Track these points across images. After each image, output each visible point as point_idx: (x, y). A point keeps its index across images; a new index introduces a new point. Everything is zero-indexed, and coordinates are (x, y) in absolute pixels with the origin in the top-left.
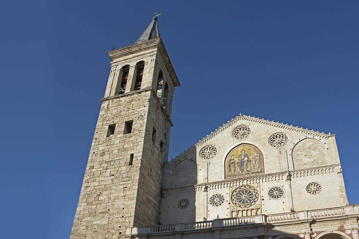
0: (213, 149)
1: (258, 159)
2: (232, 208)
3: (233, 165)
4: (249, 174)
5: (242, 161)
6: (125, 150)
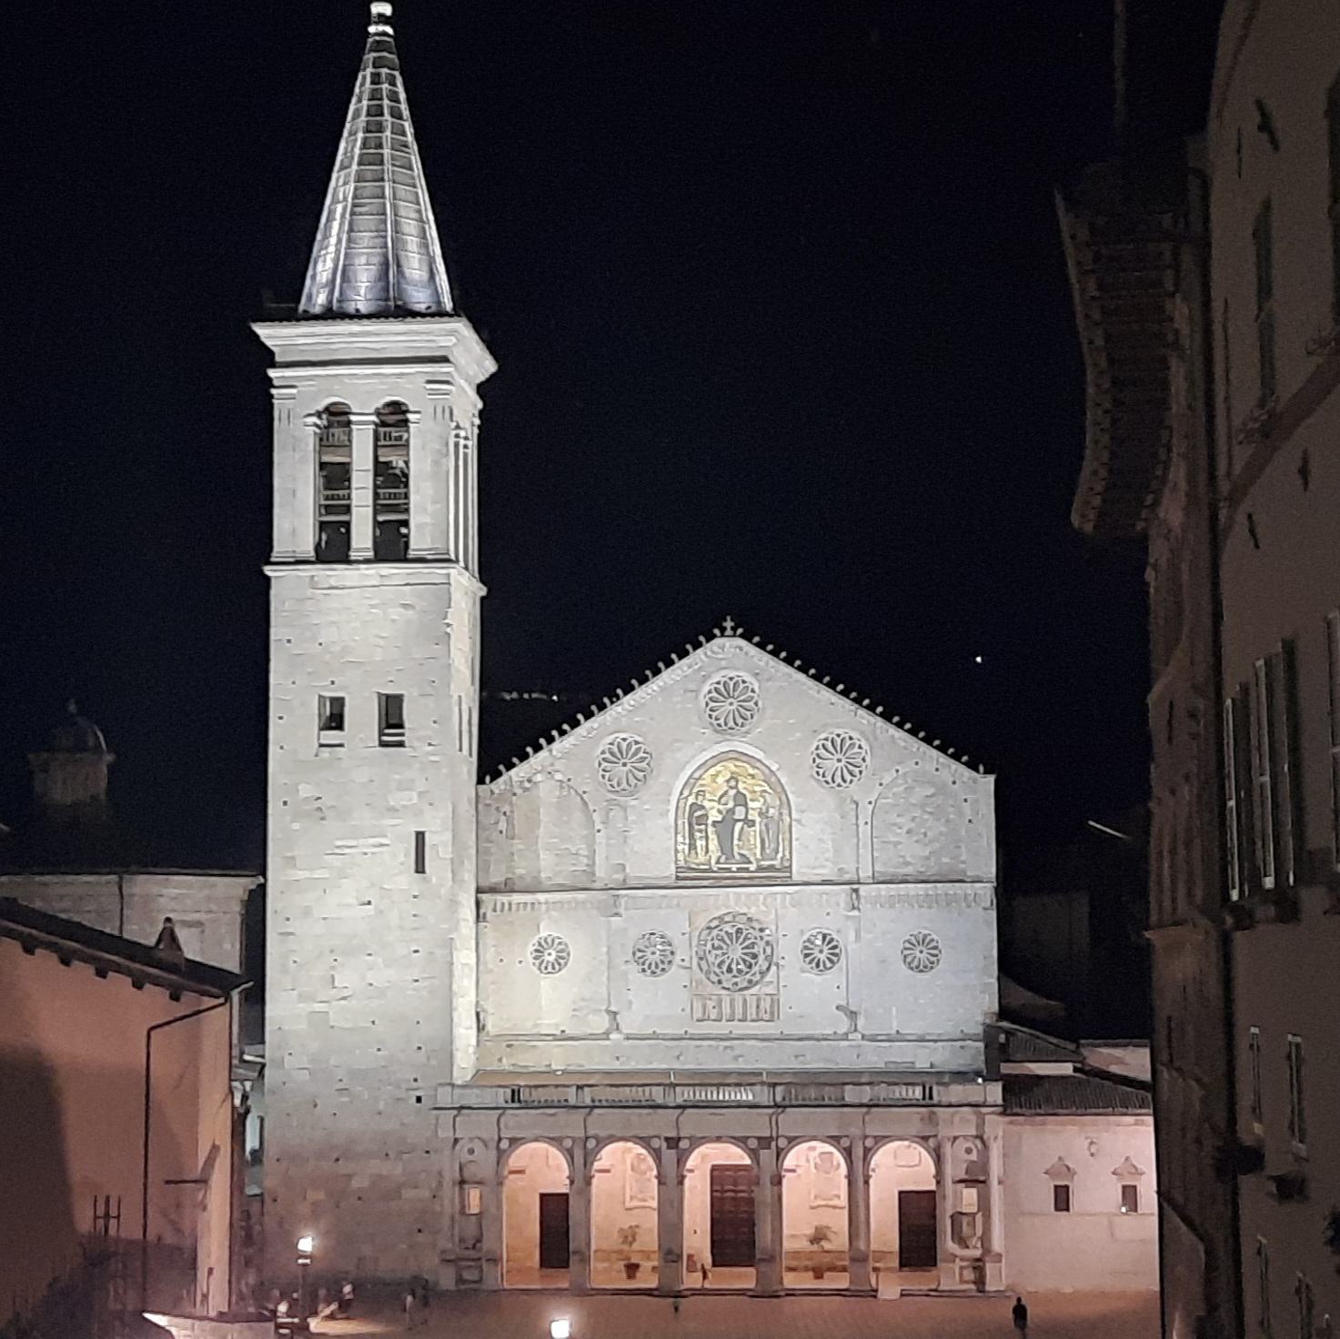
4: (747, 870)
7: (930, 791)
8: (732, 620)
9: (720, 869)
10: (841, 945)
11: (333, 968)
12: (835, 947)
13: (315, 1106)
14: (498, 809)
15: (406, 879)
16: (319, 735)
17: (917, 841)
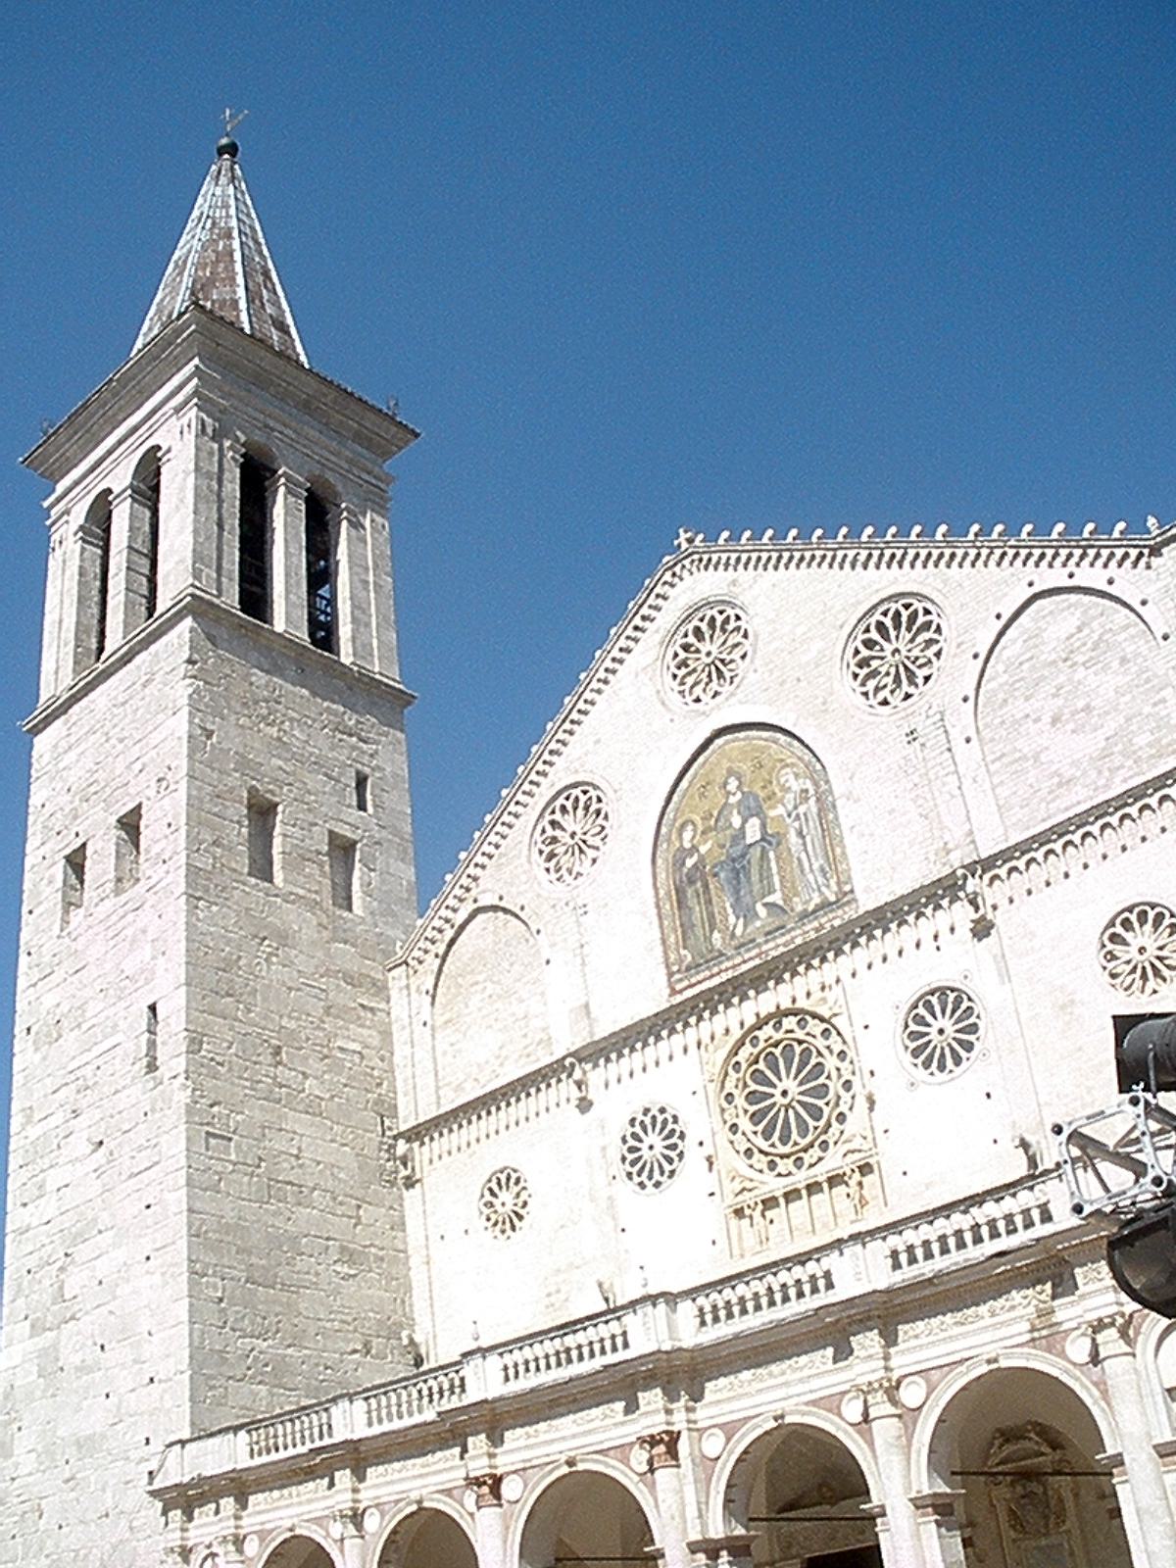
1: (815, 810)
5: (736, 851)
7: (1072, 622)
8: (686, 532)
14: (418, 990)
17: (1073, 731)
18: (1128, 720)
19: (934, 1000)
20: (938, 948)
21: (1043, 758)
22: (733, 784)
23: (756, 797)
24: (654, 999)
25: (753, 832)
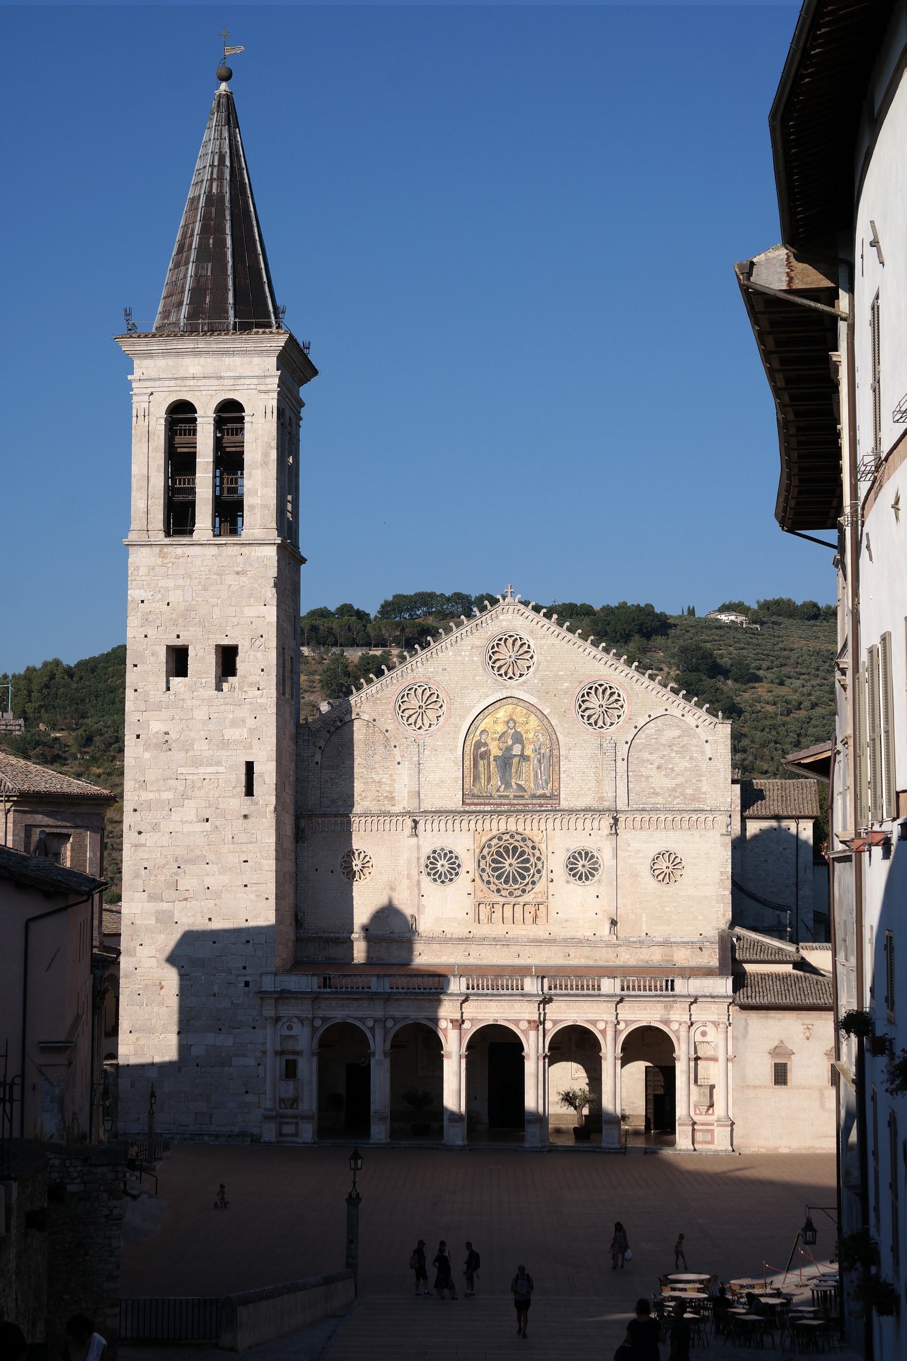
0: (431, 699)
1: (548, 754)
2: (480, 894)
3: (486, 761)
4: (522, 797)
6: (225, 744)
7: (677, 733)
9: (499, 796)
10: (600, 861)
11: (176, 874)
12: (596, 862)
13: (162, 988)
14: (314, 743)
15: (237, 802)
16: (168, 682)
18: (686, 781)
19: (583, 853)
20: (590, 835)
21: (651, 780)
22: (511, 724)
23: (521, 736)
24: (455, 802)
25: (517, 750)
